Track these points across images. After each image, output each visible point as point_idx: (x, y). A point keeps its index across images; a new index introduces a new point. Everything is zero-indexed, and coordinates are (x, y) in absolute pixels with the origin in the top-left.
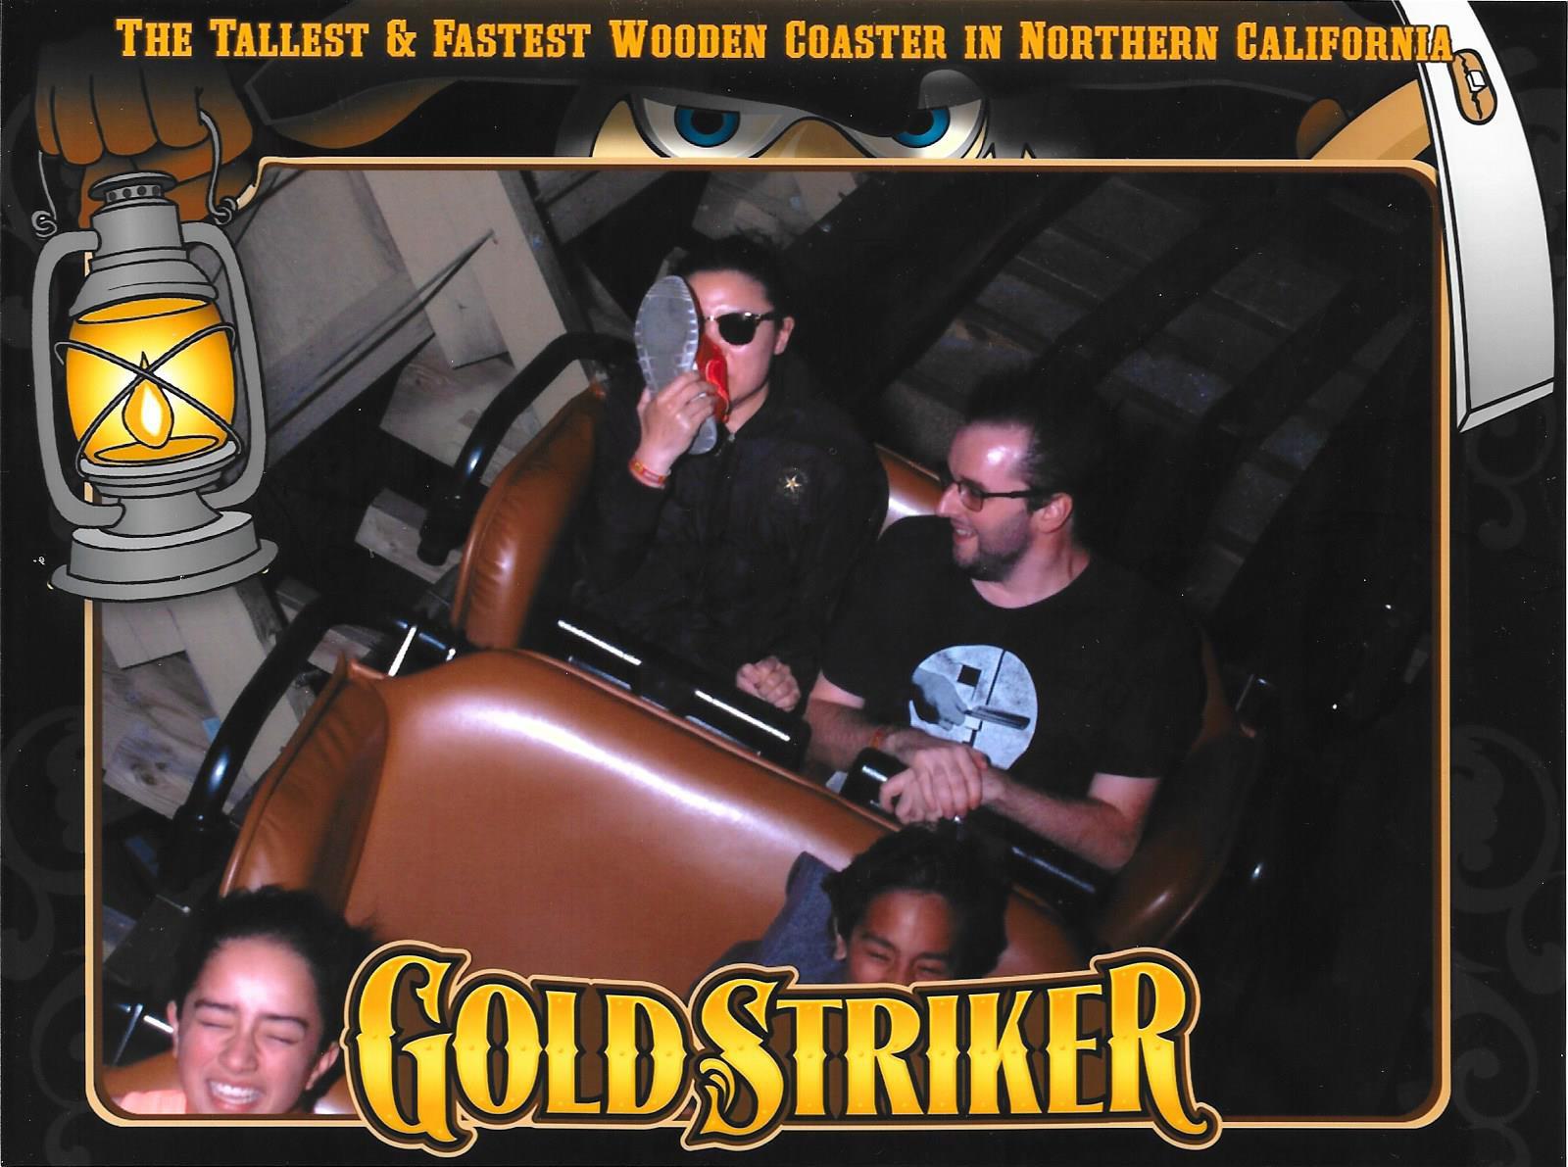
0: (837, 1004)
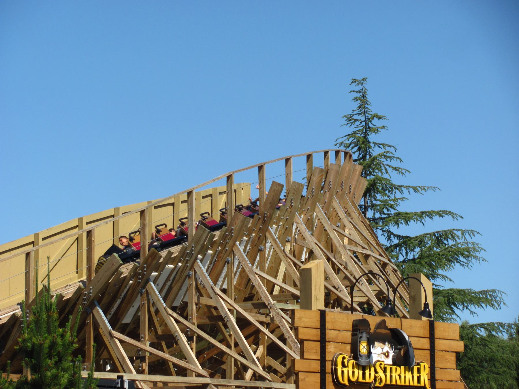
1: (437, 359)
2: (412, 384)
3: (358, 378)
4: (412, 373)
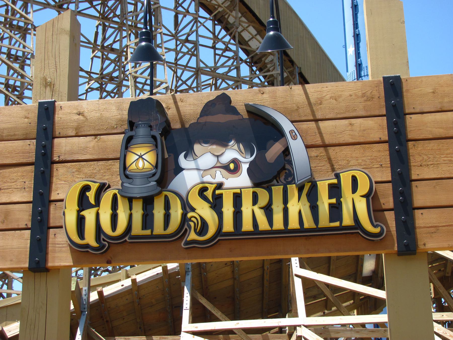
0: (238, 191)
2: (308, 223)
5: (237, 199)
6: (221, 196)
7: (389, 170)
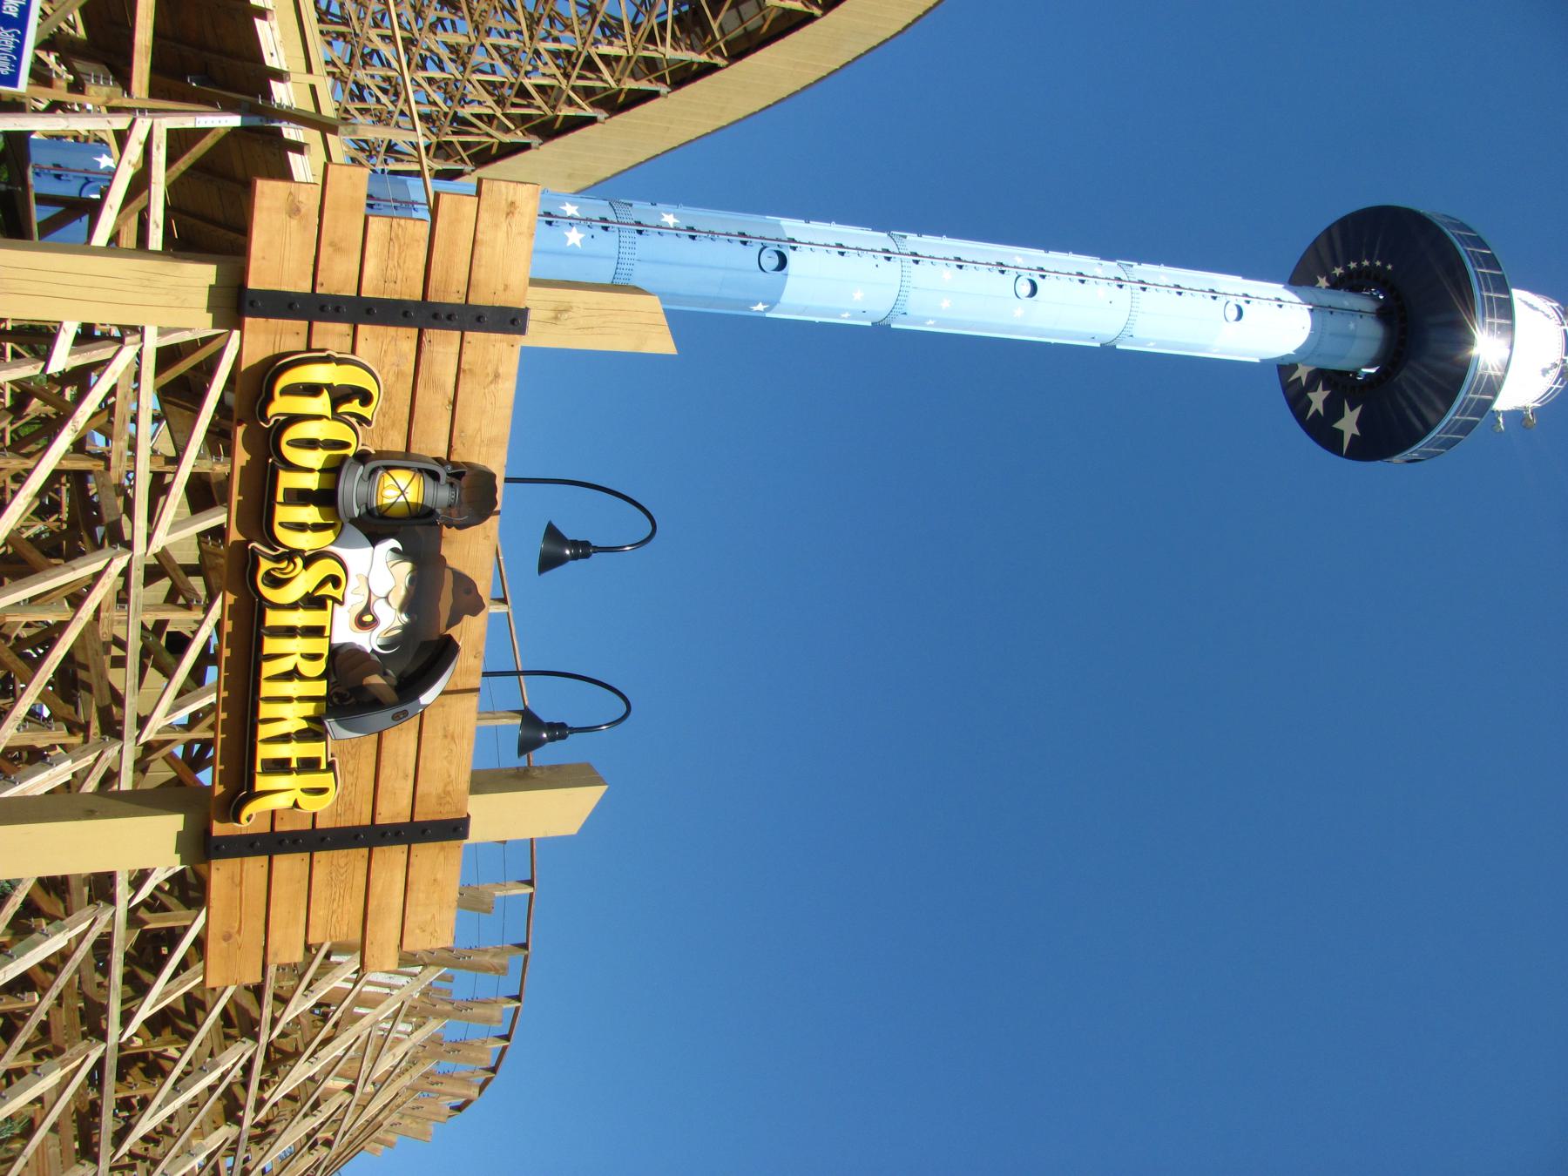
0: (327, 633)
1: (340, 856)
2: (264, 731)
3: (292, 467)
4: (302, 736)
5: (316, 632)
6: (323, 606)
7: (331, 825)
